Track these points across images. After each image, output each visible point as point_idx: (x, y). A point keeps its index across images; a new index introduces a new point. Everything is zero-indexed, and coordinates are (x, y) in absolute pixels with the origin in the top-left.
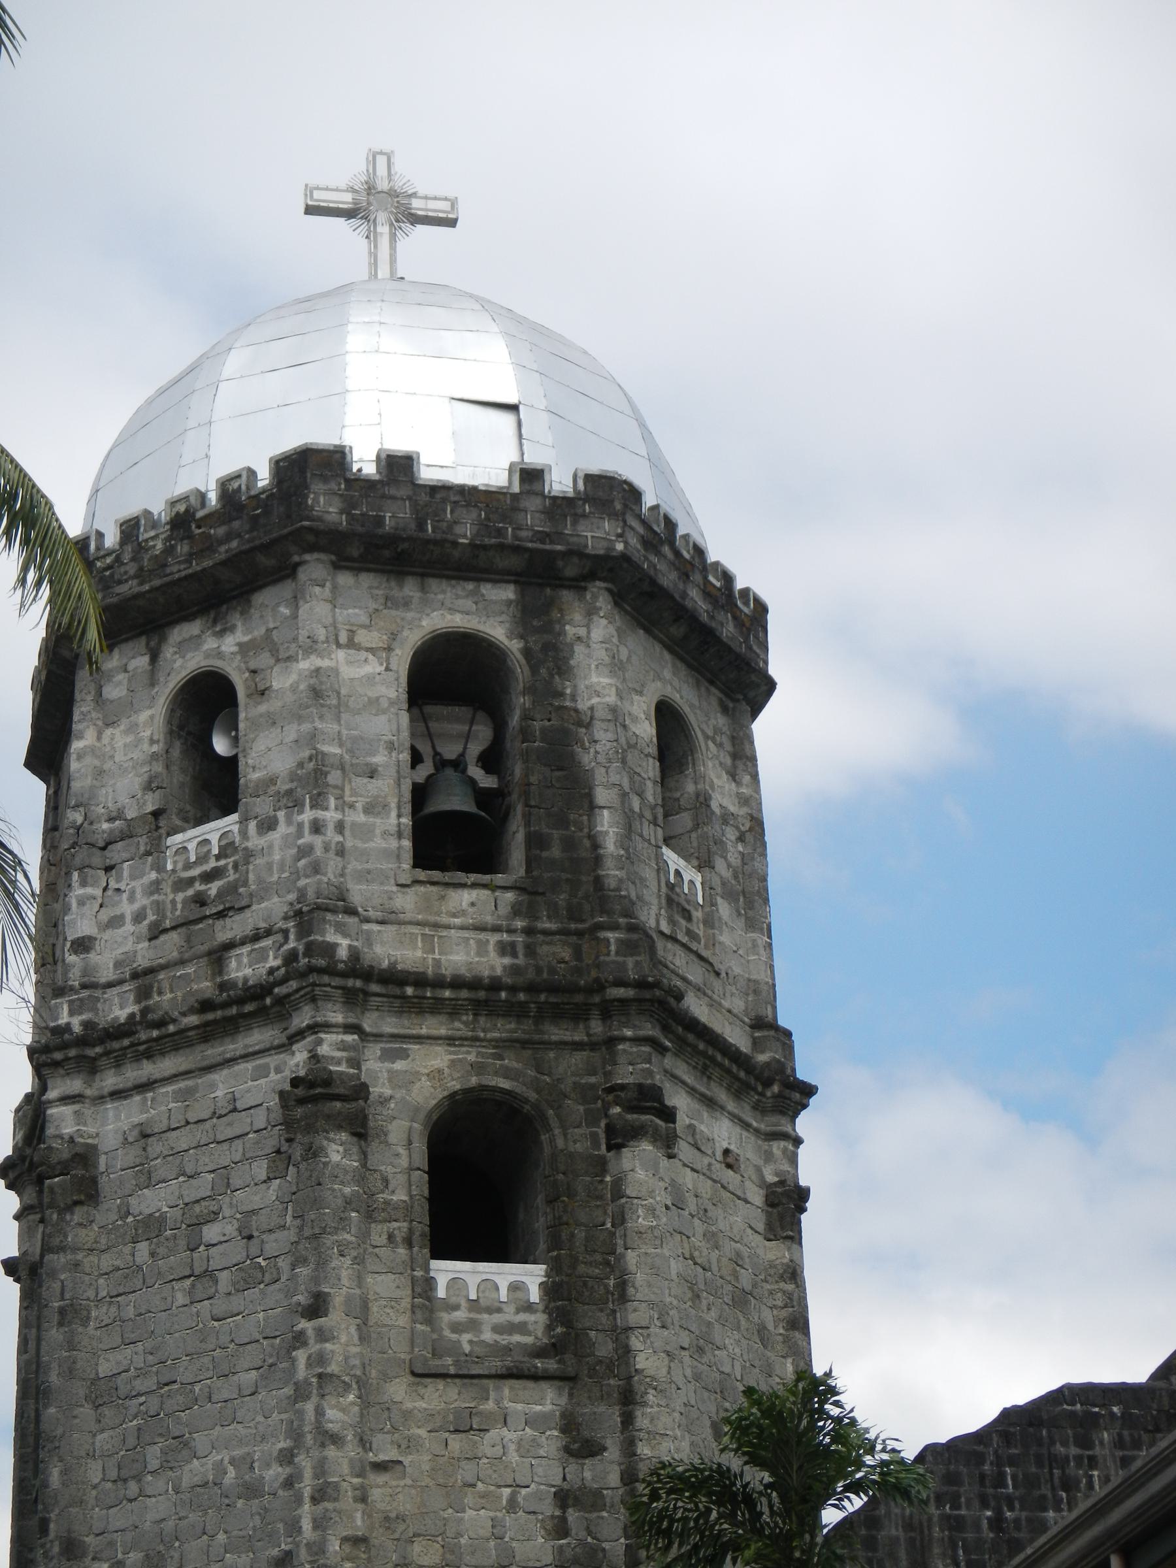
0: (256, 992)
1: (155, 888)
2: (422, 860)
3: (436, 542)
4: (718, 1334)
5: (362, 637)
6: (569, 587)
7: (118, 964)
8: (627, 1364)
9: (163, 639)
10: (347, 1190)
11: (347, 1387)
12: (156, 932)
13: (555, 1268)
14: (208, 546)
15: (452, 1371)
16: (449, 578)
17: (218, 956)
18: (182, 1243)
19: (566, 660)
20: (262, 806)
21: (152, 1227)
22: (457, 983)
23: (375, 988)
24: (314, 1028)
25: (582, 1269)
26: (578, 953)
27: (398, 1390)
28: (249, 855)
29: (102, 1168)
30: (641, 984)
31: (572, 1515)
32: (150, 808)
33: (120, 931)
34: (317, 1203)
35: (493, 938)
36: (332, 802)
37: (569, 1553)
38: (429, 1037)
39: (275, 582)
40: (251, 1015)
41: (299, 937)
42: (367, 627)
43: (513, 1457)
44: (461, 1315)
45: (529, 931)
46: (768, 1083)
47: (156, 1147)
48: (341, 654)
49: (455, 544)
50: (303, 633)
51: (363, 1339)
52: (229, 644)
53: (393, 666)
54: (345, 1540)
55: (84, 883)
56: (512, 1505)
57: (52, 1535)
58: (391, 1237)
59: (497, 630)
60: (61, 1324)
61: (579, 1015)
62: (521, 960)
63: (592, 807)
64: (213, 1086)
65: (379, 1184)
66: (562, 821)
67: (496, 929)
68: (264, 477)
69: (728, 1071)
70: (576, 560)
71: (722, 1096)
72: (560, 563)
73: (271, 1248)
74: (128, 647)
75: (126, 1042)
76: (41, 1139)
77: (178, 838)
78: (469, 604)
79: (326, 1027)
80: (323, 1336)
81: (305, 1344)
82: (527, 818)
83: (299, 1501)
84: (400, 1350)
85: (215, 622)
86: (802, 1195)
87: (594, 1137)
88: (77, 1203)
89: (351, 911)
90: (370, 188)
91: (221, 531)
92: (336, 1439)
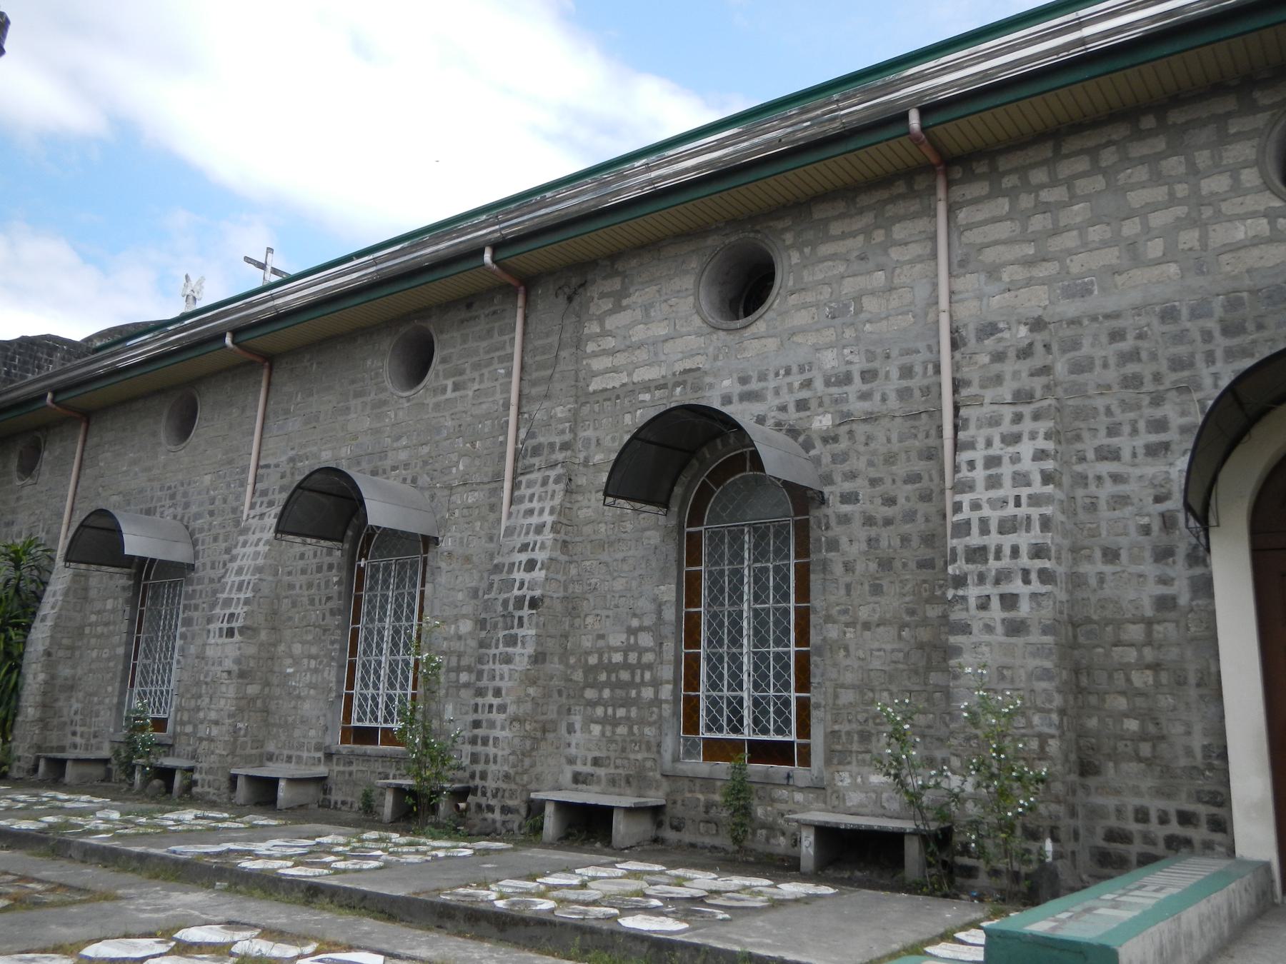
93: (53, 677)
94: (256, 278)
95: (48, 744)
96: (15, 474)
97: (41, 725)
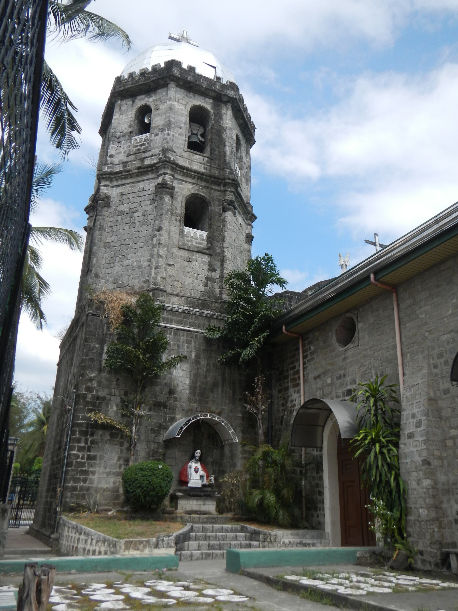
0: (151, 166)
1: (129, 146)
2: (189, 147)
3: (199, 86)
4: (237, 257)
5: (180, 101)
6: (223, 103)
7: (119, 161)
8: (223, 254)
9: (136, 98)
10: (168, 207)
11: (165, 247)
12: (128, 155)
13: (210, 233)
14: (149, 78)
15: (187, 248)
16: (200, 95)
17: (143, 160)
18: (129, 216)
19: (222, 116)
20: (156, 131)
21: (122, 213)
22: (195, 172)
23: (178, 169)
24: (164, 173)
25: (215, 234)
26: (219, 173)
27: (175, 250)
28: (151, 141)
29: (111, 200)
30: (233, 180)
31: (209, 282)
32: (129, 131)
33: (120, 155)
34: (162, 209)
35: (203, 166)
36: (172, 130)
37: (207, 290)
38: (188, 182)
39: (163, 88)
40: (149, 171)
41: (162, 155)
42: (182, 100)
43: (198, 268)
44: (189, 239)
45: (210, 166)
46: (249, 214)
47: (124, 197)
48: (176, 103)
49: (202, 87)
50: (169, 97)
51: (169, 238)
52: (151, 100)
53: (187, 108)
54: (161, 277)
55: (113, 144)
56: (197, 278)
57: (93, 273)
58: (176, 219)
59: (209, 107)
60: (99, 230)
61: (219, 184)
62: (208, 171)
63: (225, 146)
64: (139, 186)
65: (175, 209)
66: (218, 147)
67: (204, 164)
68: (162, 65)
69: (243, 208)
70: (226, 97)
71: (241, 213)
72: (223, 97)
73: (149, 218)
74: (127, 100)
75: (120, 175)
76: (99, 193)
77: (135, 137)
78: (203, 101)
79: (167, 174)
80: (160, 235)
81: (156, 237)
82: (211, 145)
83: (151, 269)
84: (176, 242)
85: (148, 95)
86: (253, 237)
87: (220, 209)
88: (105, 206)
89: (175, 152)
90: (182, 36)
91: (152, 76)
92: (161, 257)
93: (436, 483)
94: (371, 251)
95: (445, 541)
96: (336, 345)
97: (437, 523)
